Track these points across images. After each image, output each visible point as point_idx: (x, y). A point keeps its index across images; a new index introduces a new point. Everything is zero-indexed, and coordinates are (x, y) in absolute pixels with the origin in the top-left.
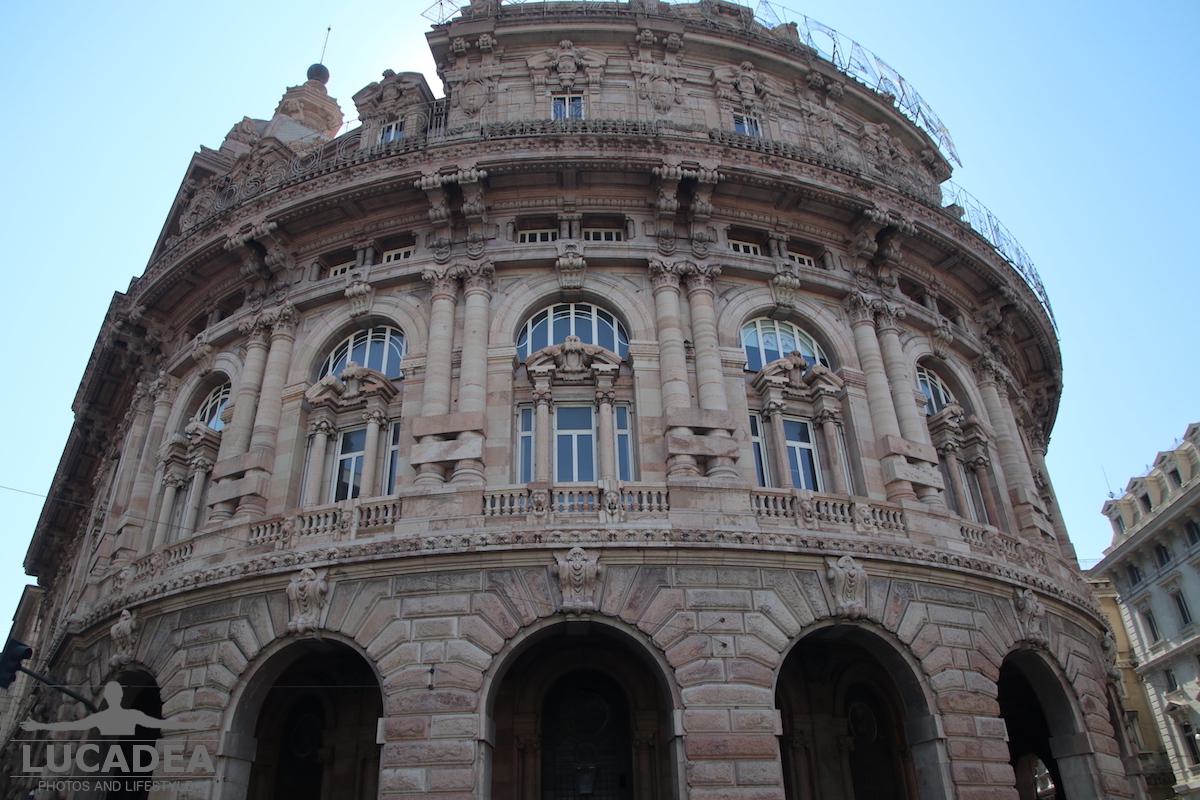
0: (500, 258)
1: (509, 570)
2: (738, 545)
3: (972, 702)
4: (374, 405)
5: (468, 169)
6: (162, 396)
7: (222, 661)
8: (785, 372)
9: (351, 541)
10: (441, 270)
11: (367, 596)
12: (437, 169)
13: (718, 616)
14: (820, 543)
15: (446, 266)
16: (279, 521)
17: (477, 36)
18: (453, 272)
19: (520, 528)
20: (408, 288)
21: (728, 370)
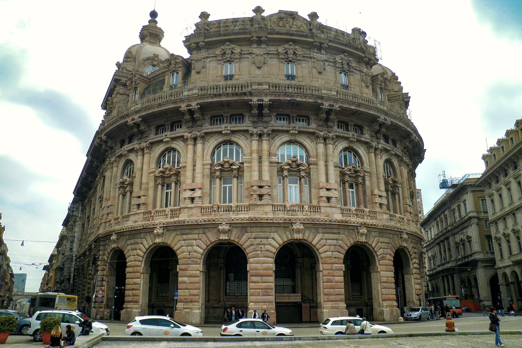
0: (206, 131)
1: (208, 228)
2: (266, 221)
3: (333, 260)
4: (173, 178)
5: (194, 105)
6: (115, 164)
7: (140, 249)
8: (289, 165)
9: (169, 220)
10: (189, 135)
11: (173, 234)
12: (185, 105)
13: (260, 240)
14: (290, 220)
15: (191, 134)
16: (150, 212)
17: (199, 43)
18: (192, 136)
19: (210, 217)
20: (181, 139)
21: (272, 164)
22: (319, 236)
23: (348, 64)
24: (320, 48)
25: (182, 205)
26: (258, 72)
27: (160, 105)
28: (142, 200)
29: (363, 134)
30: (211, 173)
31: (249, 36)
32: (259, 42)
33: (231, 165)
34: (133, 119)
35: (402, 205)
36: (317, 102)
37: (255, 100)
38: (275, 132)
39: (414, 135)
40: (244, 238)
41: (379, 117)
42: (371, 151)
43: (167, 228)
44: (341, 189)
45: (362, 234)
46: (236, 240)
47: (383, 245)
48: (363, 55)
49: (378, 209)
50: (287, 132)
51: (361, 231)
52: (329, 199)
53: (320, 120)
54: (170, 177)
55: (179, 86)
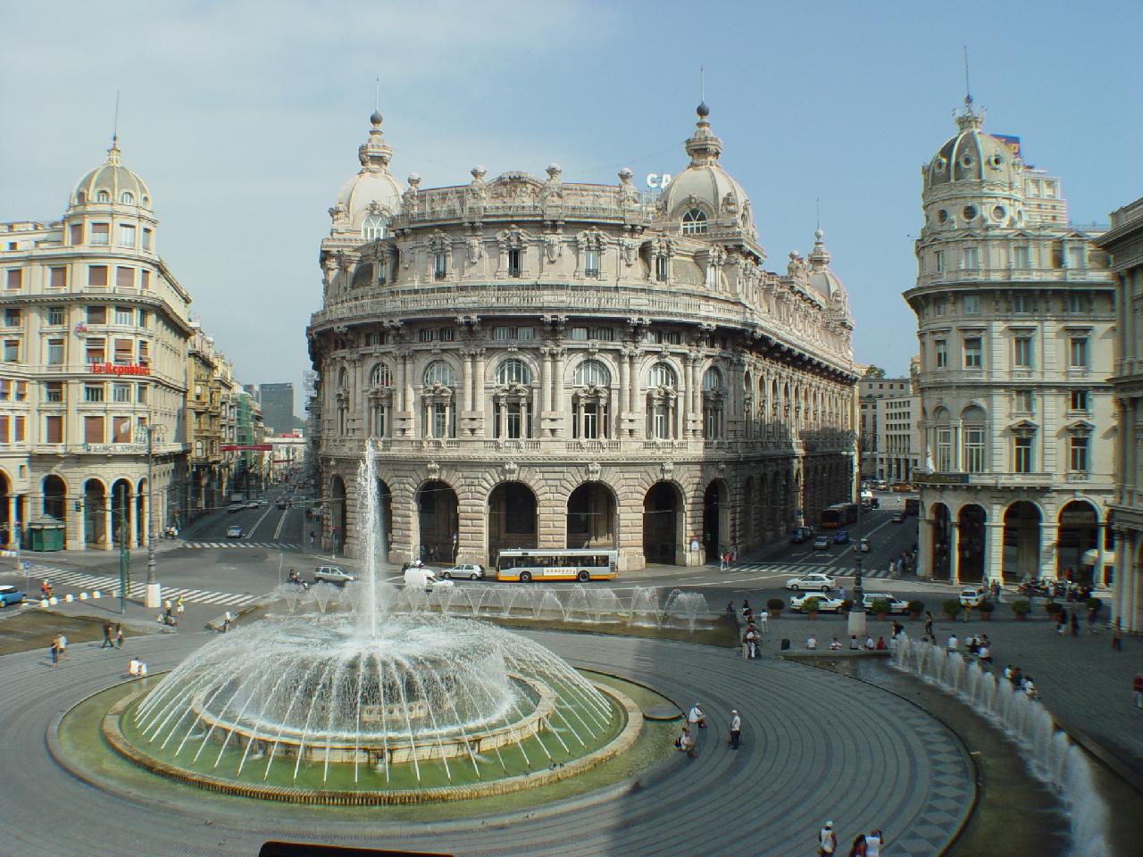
3: (554, 503)
6: (331, 368)
23: (598, 240)
24: (554, 226)
25: (393, 438)
28: (357, 425)
33: (443, 391)
37: (461, 319)
39: (705, 324)
40: (454, 479)
48: (622, 222)
51: (591, 468)
52: (553, 431)
55: (388, 281)
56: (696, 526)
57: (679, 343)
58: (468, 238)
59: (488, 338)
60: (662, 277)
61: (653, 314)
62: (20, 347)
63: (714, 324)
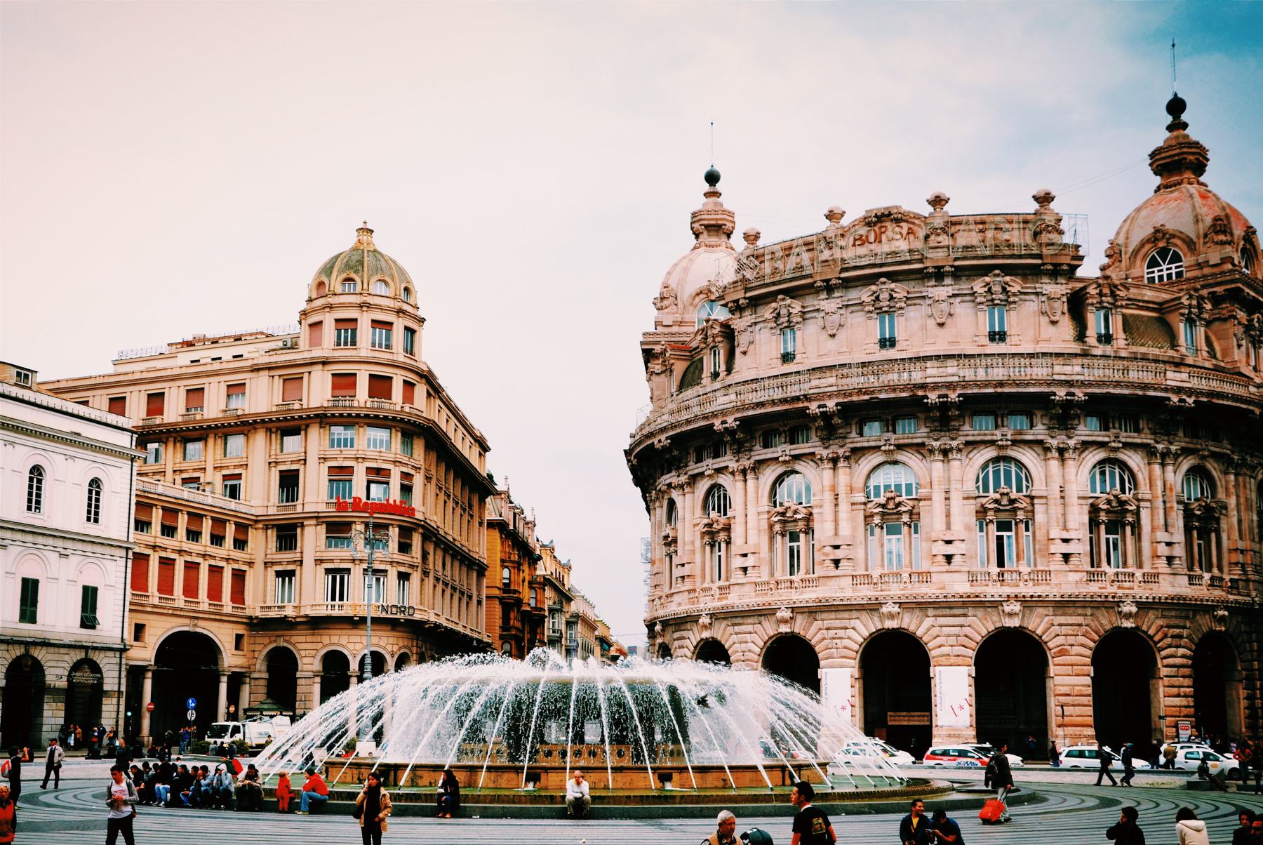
5: (730, 419)
8: (883, 506)
9: (717, 604)
11: (724, 623)
22: (928, 622)
23: (1004, 289)
24: (938, 275)
25: (732, 581)
26: (832, 344)
27: (688, 422)
28: (686, 571)
29: (1032, 427)
30: (771, 526)
31: (809, 281)
32: (829, 288)
33: (796, 512)
34: (660, 441)
35: (1146, 544)
36: (915, 395)
37: (813, 407)
38: (858, 452)
39: (1175, 399)
41: (1055, 394)
42: (1049, 455)
43: (715, 616)
44: (984, 534)
45: (1010, 615)
46: (802, 633)
47: (1064, 630)
48: (1039, 261)
49: (1057, 564)
50: (878, 448)
52: (949, 558)
53: (933, 421)
54: (718, 532)
56: (1183, 701)
57: (1137, 430)
58: (822, 303)
59: (854, 435)
60: (1106, 338)
61: (1090, 384)
62: (242, 482)
63: (1190, 400)
